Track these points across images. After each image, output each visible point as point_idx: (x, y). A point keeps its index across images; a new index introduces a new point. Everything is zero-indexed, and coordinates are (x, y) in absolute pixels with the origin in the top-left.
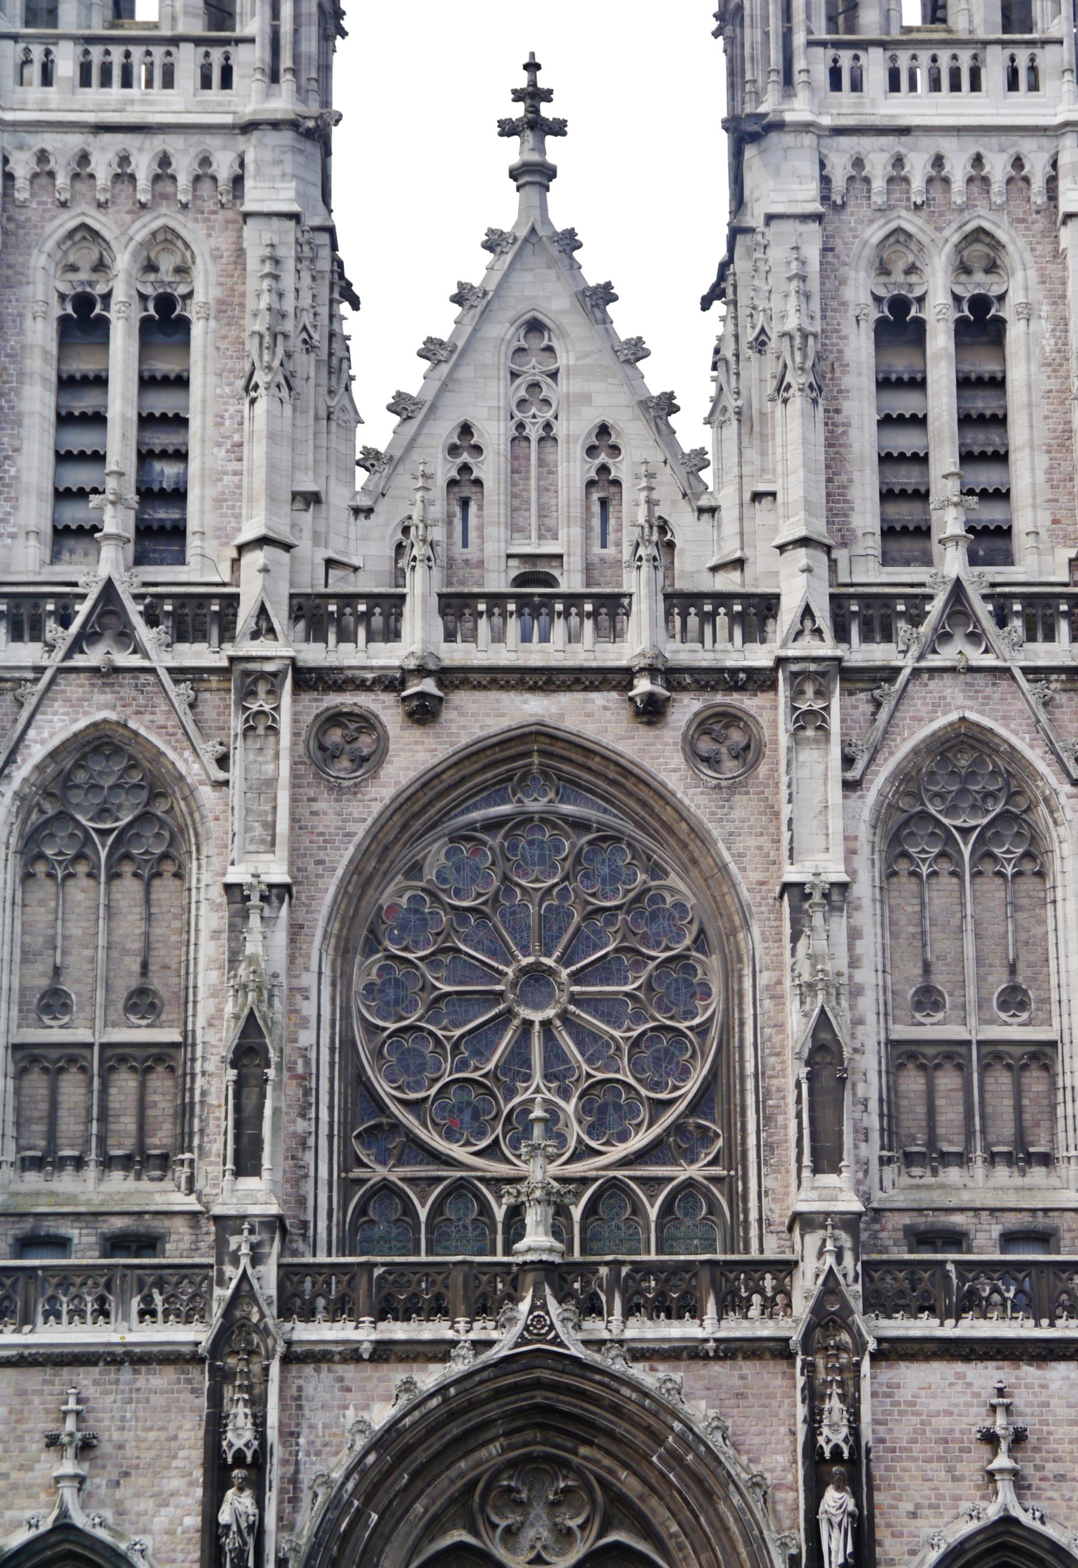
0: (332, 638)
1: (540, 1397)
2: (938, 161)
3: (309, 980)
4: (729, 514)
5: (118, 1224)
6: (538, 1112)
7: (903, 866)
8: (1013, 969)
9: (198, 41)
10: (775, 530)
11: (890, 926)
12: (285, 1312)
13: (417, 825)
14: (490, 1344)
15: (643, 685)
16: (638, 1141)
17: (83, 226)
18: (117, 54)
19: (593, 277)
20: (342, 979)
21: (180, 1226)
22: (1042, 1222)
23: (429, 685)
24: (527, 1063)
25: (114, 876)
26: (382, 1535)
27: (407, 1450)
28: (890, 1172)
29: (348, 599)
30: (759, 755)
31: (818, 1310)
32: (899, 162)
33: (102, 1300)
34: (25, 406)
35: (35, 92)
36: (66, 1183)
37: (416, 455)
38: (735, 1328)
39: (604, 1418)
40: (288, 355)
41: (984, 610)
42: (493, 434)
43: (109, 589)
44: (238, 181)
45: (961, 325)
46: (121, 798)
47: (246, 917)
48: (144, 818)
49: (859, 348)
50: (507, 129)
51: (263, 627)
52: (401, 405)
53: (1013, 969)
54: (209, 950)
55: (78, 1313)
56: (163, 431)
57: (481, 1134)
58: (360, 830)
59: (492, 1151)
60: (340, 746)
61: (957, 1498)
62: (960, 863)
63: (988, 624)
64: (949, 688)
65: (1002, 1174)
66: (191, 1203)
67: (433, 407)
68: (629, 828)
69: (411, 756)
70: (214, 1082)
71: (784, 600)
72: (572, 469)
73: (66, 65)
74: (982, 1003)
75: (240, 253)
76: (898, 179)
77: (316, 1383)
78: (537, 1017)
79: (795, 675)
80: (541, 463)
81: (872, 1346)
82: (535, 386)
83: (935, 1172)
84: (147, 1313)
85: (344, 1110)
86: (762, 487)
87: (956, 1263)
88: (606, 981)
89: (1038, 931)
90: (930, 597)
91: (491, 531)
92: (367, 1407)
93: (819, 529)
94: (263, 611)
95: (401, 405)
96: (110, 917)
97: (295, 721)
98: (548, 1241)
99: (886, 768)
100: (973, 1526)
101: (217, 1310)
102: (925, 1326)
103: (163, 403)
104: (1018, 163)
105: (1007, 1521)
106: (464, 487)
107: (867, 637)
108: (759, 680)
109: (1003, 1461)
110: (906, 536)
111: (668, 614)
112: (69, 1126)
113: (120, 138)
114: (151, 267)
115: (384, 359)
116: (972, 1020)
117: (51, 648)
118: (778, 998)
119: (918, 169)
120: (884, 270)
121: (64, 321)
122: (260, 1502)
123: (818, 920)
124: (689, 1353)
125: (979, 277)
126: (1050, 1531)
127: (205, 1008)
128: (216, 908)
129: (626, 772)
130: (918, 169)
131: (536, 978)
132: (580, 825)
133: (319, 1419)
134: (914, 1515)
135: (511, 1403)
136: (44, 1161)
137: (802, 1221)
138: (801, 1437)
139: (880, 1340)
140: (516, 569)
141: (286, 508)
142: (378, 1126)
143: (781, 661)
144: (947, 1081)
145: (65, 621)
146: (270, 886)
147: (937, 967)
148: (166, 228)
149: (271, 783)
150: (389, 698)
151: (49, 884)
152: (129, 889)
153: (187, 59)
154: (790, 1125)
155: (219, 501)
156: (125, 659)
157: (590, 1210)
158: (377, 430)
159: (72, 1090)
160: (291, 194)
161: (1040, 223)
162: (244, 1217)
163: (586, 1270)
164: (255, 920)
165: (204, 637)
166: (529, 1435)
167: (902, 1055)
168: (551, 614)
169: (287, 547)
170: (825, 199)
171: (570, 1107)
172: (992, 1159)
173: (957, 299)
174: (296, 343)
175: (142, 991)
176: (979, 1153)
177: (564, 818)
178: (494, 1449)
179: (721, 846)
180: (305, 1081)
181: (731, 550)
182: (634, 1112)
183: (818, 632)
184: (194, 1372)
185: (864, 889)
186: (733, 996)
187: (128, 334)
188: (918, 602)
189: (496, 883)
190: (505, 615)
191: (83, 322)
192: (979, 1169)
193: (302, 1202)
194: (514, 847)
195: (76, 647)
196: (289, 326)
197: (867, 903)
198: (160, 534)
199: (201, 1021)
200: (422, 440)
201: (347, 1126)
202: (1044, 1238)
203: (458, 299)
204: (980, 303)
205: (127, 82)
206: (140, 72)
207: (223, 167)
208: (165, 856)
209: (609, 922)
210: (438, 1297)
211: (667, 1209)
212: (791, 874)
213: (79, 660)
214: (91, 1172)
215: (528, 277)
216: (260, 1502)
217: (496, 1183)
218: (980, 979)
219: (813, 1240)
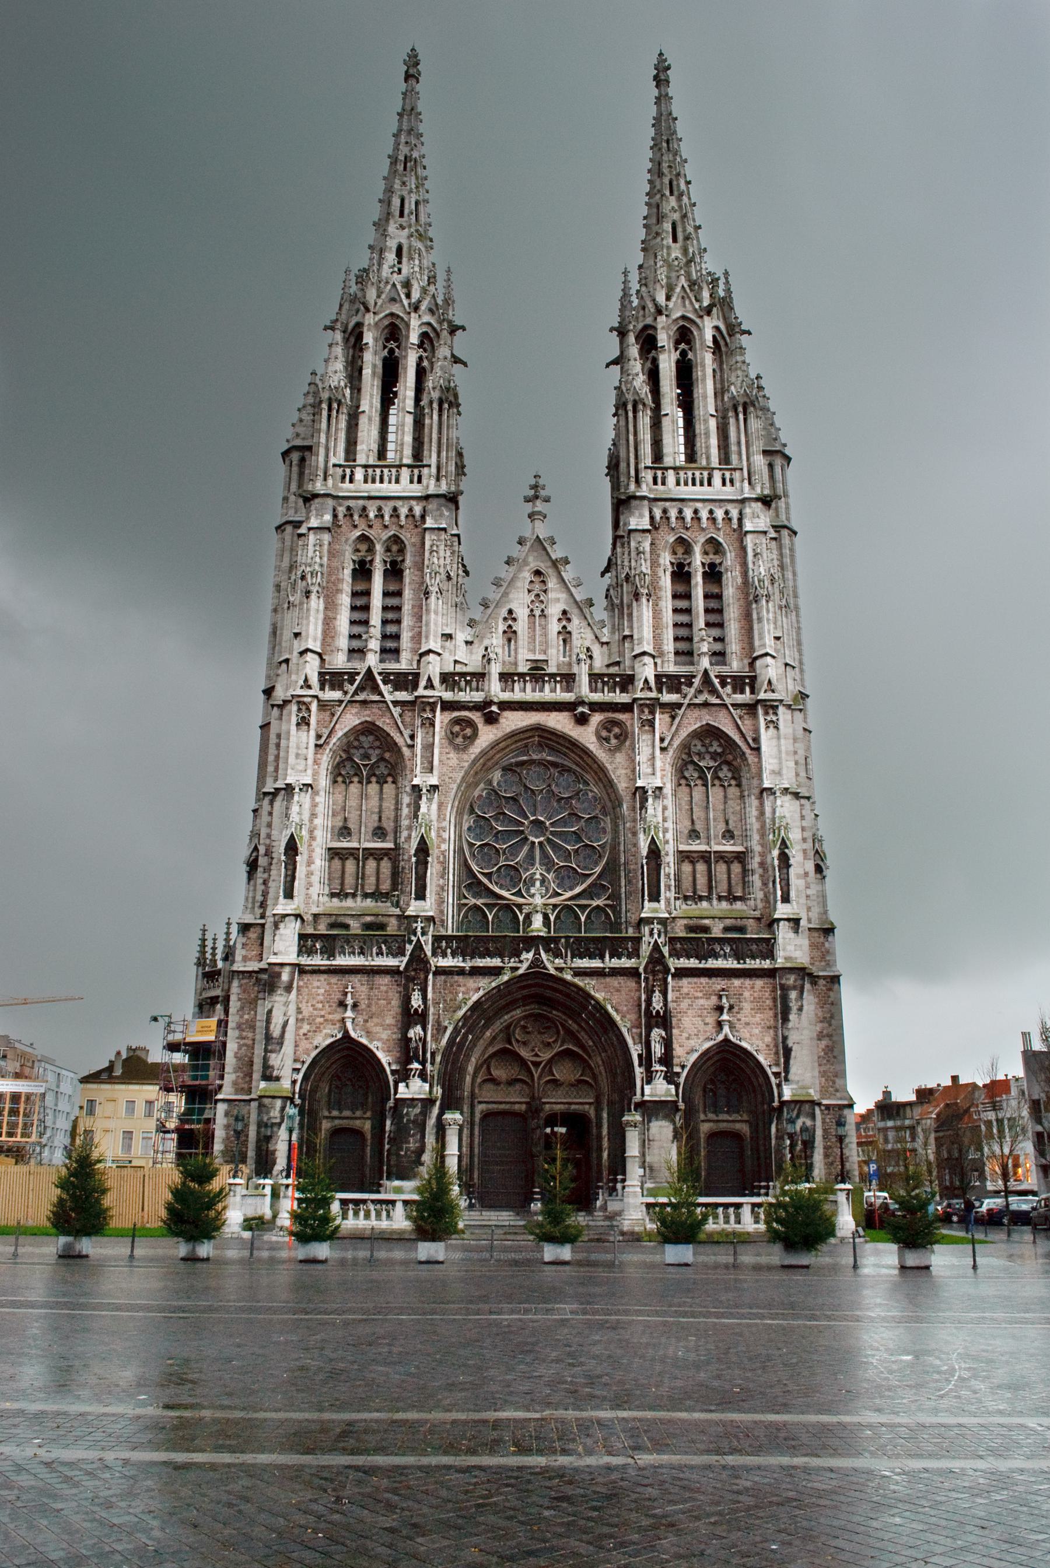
2: (696, 512)
3: (445, 824)
5: (368, 919)
6: (538, 876)
7: (683, 782)
8: (727, 823)
9: (408, 466)
10: (633, 650)
11: (677, 805)
12: (434, 954)
13: (490, 764)
14: (517, 969)
16: (578, 890)
18: (378, 471)
20: (459, 824)
21: (393, 922)
22: (739, 923)
23: (494, 708)
25: (369, 782)
26: (474, 1043)
28: (678, 903)
29: (463, 675)
30: (626, 737)
31: (651, 956)
32: (680, 511)
35: (347, 485)
36: (349, 903)
38: (615, 963)
41: (716, 681)
43: (369, 670)
44: (423, 517)
46: (371, 751)
47: (420, 797)
48: (382, 759)
49: (666, 582)
50: (528, 500)
53: (727, 823)
54: (405, 811)
56: (392, 612)
57: (514, 887)
58: (466, 764)
59: (519, 894)
63: (718, 686)
65: (724, 904)
66: (397, 911)
68: (574, 767)
69: (487, 735)
72: (554, 627)
73: (359, 474)
74: (716, 836)
75: (423, 544)
76: (681, 518)
78: (537, 841)
82: (538, 595)
84: (380, 953)
90: (694, 677)
91: (520, 651)
93: (649, 648)
94: (429, 679)
99: (677, 743)
100: (712, 1043)
101: (408, 953)
102: (693, 963)
103: (392, 602)
104: (727, 513)
105: (726, 1040)
108: (627, 708)
109: (725, 1017)
112: (350, 880)
117: (346, 693)
119: (688, 514)
122: (424, 1029)
123: (650, 800)
126: (744, 1044)
127: (405, 834)
130: (688, 514)
131: (537, 823)
134: (688, 1039)
135: (525, 992)
136: (339, 894)
141: (439, 640)
143: (635, 700)
145: (352, 682)
147: (697, 822)
148: (394, 535)
150: (479, 714)
151: (343, 786)
152: (373, 788)
153: (405, 473)
155: (413, 638)
159: (350, 866)
161: (736, 535)
163: (556, 940)
164: (424, 798)
167: (684, 856)
168: (544, 681)
169: (439, 654)
171: (550, 876)
172: (720, 898)
173: (703, 564)
175: (379, 828)
178: (518, 1011)
180: (444, 864)
183: (650, 689)
184: (397, 977)
185: (668, 790)
188: (689, 679)
190: (525, 682)
191: (362, 571)
192: (715, 902)
193: (442, 912)
195: (355, 693)
196: (442, 570)
198: (390, 652)
201: (460, 883)
204: (712, 565)
205: (382, 482)
206: (386, 478)
207: (418, 510)
211: (588, 917)
212: (639, 784)
213: (357, 698)
214: (359, 899)
216: (424, 1029)
217: (520, 906)
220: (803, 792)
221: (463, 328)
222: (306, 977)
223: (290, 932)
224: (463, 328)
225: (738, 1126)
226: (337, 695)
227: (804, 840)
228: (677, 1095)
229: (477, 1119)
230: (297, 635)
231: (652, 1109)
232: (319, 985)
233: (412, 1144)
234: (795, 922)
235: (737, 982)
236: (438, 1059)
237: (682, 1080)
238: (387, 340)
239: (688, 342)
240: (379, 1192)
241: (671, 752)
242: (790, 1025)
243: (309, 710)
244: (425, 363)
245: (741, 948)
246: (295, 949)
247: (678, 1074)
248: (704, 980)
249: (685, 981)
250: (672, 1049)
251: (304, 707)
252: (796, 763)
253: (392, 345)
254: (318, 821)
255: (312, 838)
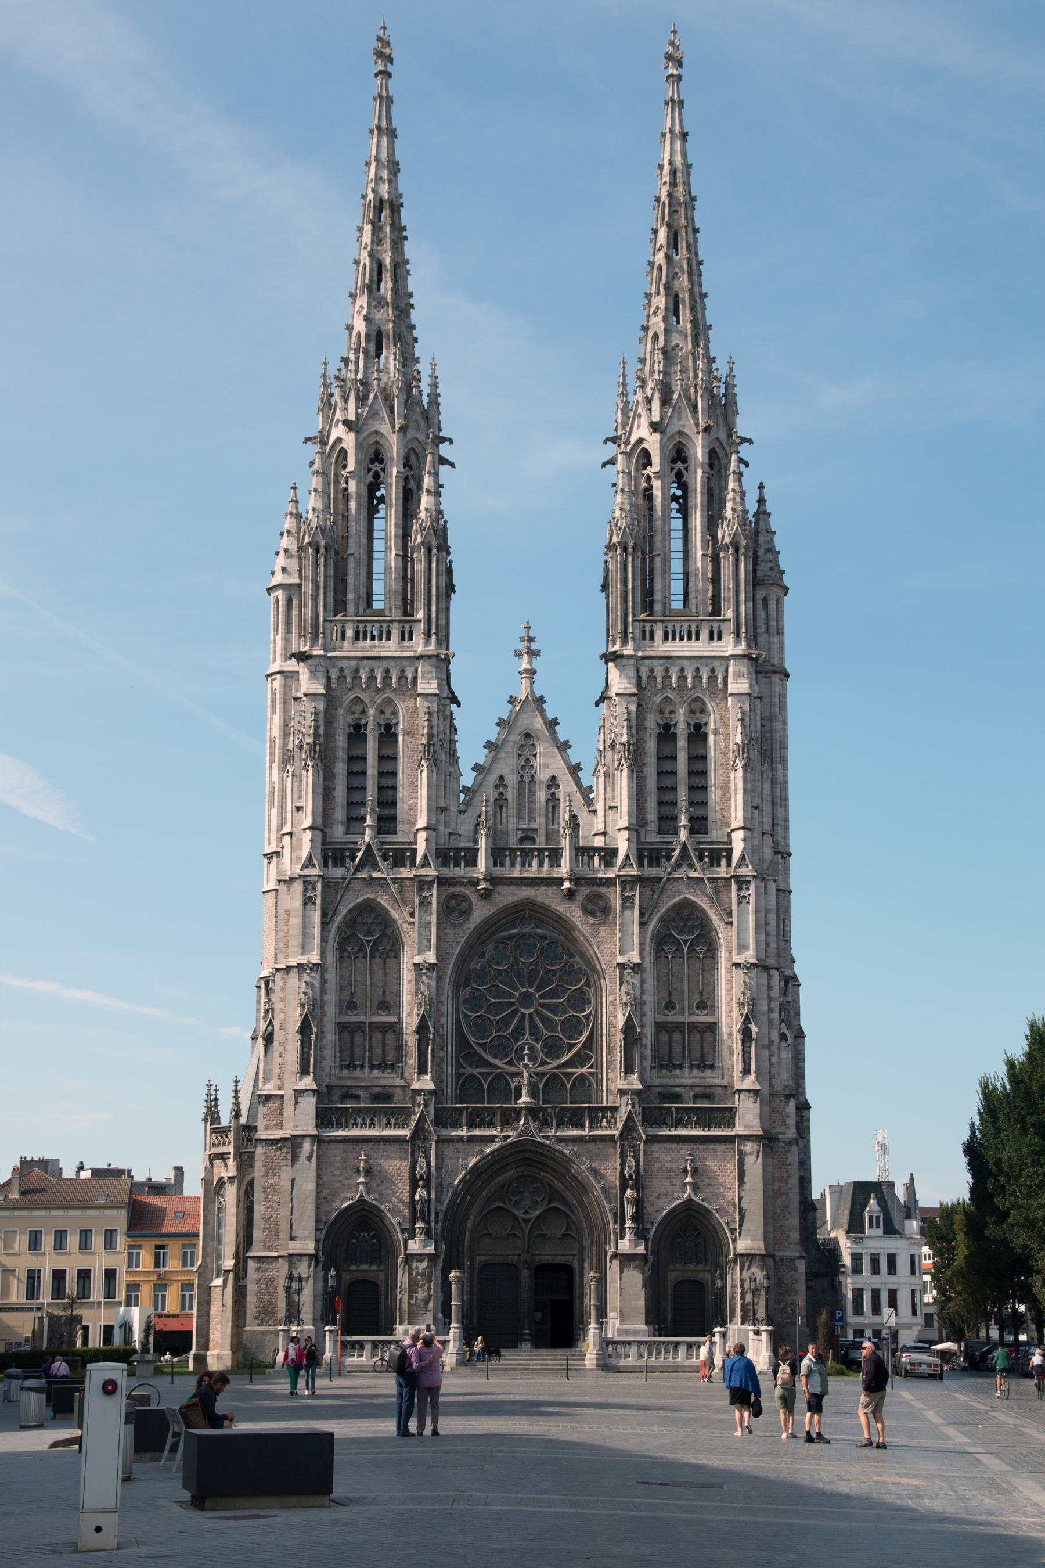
0: (451, 866)
1: (527, 1155)
3: (444, 998)
4: (600, 813)
5: (377, 1090)
11: (658, 979)
14: (509, 1137)
15: (567, 885)
17: (357, 697)
19: (550, 717)
20: (456, 996)
21: (399, 1091)
22: (708, 1090)
24: (523, 1029)
25: (372, 957)
27: (481, 1173)
28: (654, 1072)
29: (457, 850)
33: (372, 1120)
34: (336, 771)
36: (358, 1073)
37: (483, 789)
39: (549, 1162)
40: (435, 752)
41: (693, 855)
42: (511, 780)
45: (690, 735)
49: (651, 745)
51: (425, 863)
52: (477, 768)
53: (701, 994)
55: (364, 1124)
60: (453, 908)
61: (673, 1192)
62: (683, 953)
64: (681, 886)
65: (695, 1072)
67: (489, 770)
69: (481, 912)
70: (411, 1040)
71: (620, 851)
72: (542, 795)
74: (690, 1007)
77: (449, 1151)
79: (622, 882)
80: (530, 791)
81: (644, 1138)
83: (671, 1071)
85: (457, 1047)
86: (613, 804)
87: (676, 1108)
88: (552, 998)
89: (711, 979)
90: (675, 850)
91: (511, 820)
92: (466, 1159)
95: (477, 768)
96: (371, 973)
97: (438, 898)
98: (528, 1099)
101: (413, 1124)
105: (690, 1200)
106: (500, 802)
107: (650, 865)
108: (610, 882)
109: (689, 1179)
110: (667, 823)
111: (576, 855)
112: (358, 1052)
113: (371, 662)
114: (382, 712)
115: (470, 752)
116: (686, 1014)
117: (348, 870)
118: (614, 1006)
120: (662, 712)
121: (350, 735)
122: (429, 1193)
124: (580, 1140)
125: (698, 715)
128: (409, 971)
129: (560, 918)
132: (543, 937)
133: (450, 1163)
134: (658, 1198)
137: (623, 1092)
138: (618, 1171)
139: (647, 1136)
140: (520, 834)
142: (469, 1053)
144: (677, 1036)
145: (353, 859)
146: (430, 964)
148: (388, 697)
149: (430, 923)
150: (473, 889)
152: (378, 962)
154: (619, 1055)
156: (376, 875)
157: (546, 1085)
158: (468, 778)
160: (436, 686)
162: (421, 1090)
165: (404, 865)
166: (523, 1168)
169: (435, 830)
170: (638, 684)
172: (691, 1067)
173: (689, 724)
174: (438, 747)
175: (383, 1002)
176: (687, 1065)
177: (538, 935)
179: (595, 947)
181: (600, 827)
182: (562, 1048)
184: (405, 1146)
185: (647, 964)
186: (598, 1004)
187: (374, 740)
189: (512, 959)
194: (519, 945)
197: (648, 969)
198: (387, 822)
199: (405, 1014)
200: (485, 783)
201: (457, 1052)
202: (709, 1097)
203: (498, 724)
208: (391, 950)
209: (554, 975)
210: (491, 1120)
212: (620, 959)
214: (367, 1070)
215: (525, 716)
216: (429, 1193)
218: (689, 998)
219: (625, 1099)
220: (771, 962)
221: (451, 441)
222: (324, 1146)
223: (309, 1104)
224: (451, 441)
225: (701, 1275)
226: (339, 872)
227: (771, 1010)
228: (646, 1249)
229: (476, 1270)
230: (298, 809)
231: (626, 1260)
232: (336, 1154)
233: (421, 1295)
234: (756, 1093)
235: (701, 1147)
236: (441, 1217)
237: (651, 1235)
238: (372, 462)
239: (685, 461)
240: (391, 1335)
241: (651, 928)
242: (746, 1187)
243: (314, 889)
244: (412, 485)
245: (707, 1118)
246: (313, 1121)
247: (648, 1230)
248: (675, 1145)
249: (656, 1147)
250: (643, 1208)
251: (310, 887)
252: (767, 934)
253: (377, 467)
254: (327, 998)
255: (324, 1014)
